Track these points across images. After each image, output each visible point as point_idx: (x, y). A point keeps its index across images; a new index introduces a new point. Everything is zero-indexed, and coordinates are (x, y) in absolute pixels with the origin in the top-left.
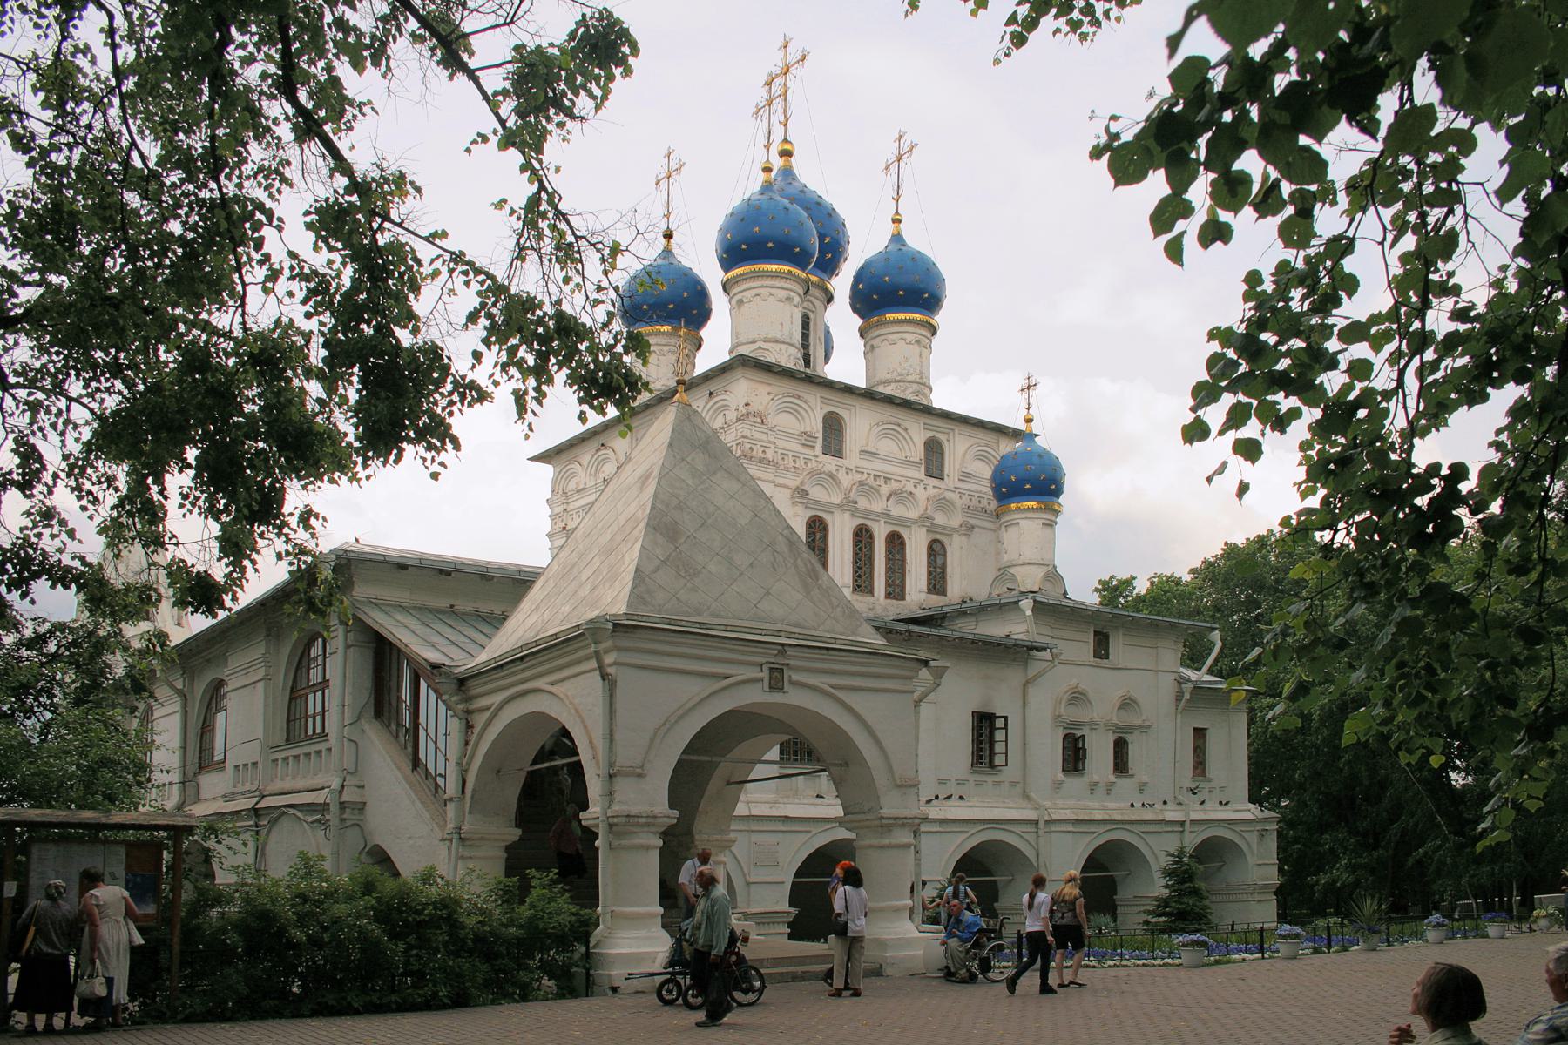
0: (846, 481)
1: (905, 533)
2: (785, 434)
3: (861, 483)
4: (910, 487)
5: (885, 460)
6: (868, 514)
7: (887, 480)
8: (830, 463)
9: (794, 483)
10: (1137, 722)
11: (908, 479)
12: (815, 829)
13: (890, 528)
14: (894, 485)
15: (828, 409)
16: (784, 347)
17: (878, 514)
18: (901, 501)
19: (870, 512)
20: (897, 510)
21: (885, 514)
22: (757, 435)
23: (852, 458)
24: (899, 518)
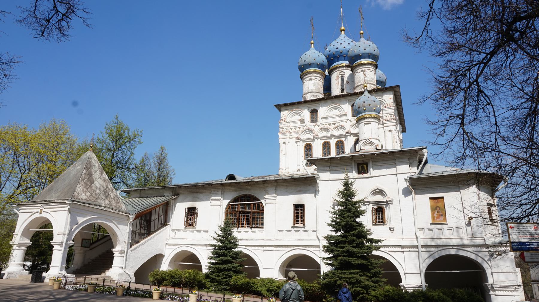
0: (316, 129)
1: (343, 139)
2: (294, 122)
3: (321, 129)
4: (343, 123)
7: (334, 124)
9: (296, 136)
10: (385, 200)
11: (342, 121)
12: (175, 247)
14: (337, 125)
15: (311, 109)
19: (326, 137)
20: (336, 133)
21: (332, 136)
23: (320, 121)
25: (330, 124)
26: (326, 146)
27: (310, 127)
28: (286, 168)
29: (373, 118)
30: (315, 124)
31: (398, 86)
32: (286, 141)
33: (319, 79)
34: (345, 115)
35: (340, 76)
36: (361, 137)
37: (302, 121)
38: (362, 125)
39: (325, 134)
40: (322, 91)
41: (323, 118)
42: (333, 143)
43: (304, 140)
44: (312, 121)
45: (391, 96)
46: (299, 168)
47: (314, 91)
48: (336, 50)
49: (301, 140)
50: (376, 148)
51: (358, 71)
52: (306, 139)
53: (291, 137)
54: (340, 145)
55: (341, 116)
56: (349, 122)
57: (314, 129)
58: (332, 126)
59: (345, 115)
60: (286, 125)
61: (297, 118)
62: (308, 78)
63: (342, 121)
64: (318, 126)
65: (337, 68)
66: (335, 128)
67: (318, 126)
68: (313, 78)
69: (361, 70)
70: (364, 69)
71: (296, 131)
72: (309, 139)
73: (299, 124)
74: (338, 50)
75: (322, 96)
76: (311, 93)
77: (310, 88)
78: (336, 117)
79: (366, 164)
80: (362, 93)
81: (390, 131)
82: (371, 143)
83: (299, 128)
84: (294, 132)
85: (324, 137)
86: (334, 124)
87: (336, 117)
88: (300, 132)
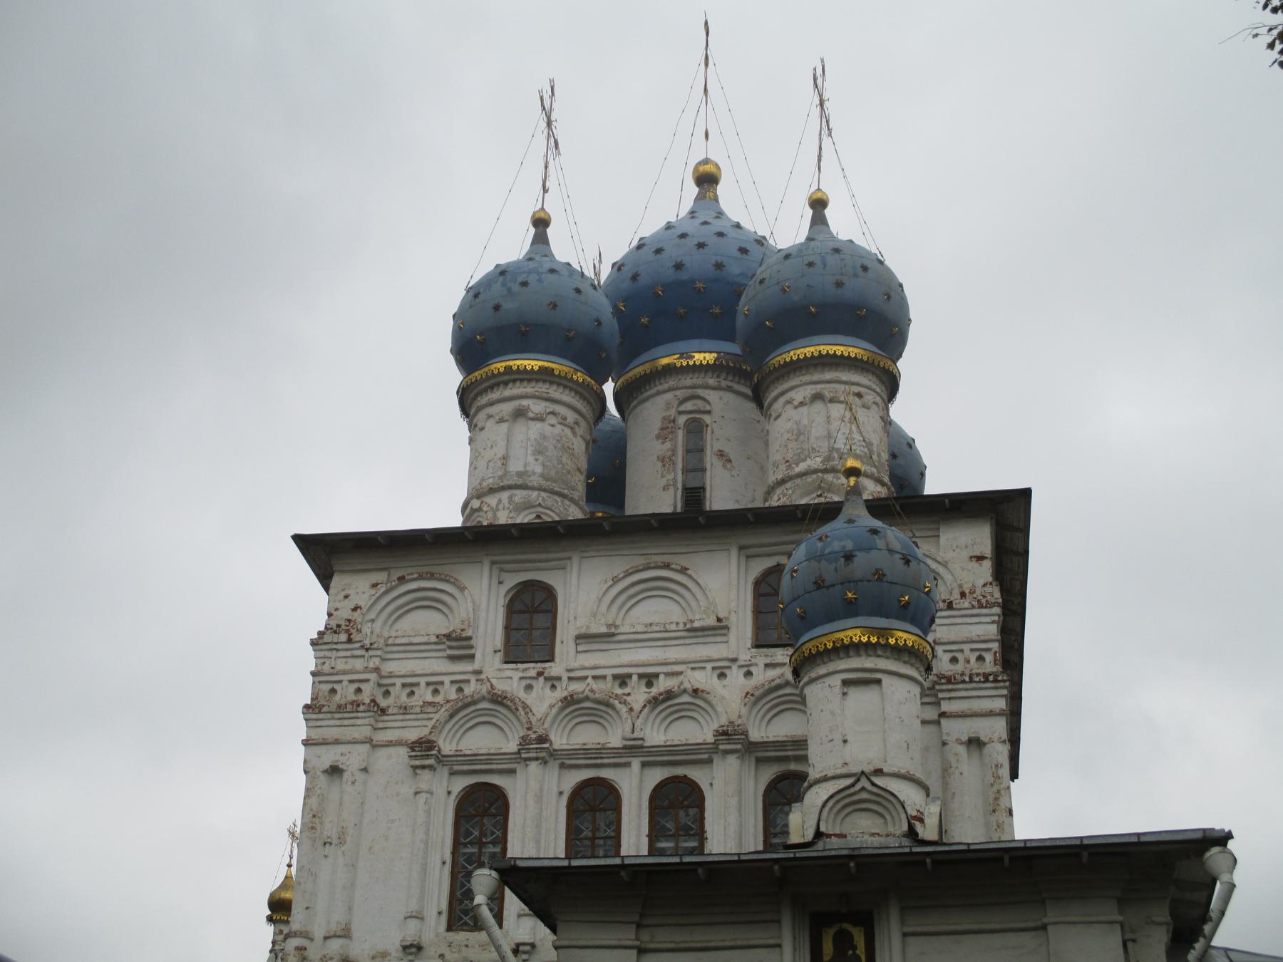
0: (542, 701)
1: (697, 774)
2: (411, 648)
4: (701, 679)
5: (637, 640)
6: (595, 755)
8: (510, 680)
9: (412, 735)
11: (697, 665)
13: (657, 776)
14: (663, 684)
15: (513, 580)
16: (505, 495)
17: (616, 752)
18: (681, 713)
20: (656, 735)
21: (634, 748)
22: (340, 665)
23: (566, 656)
24: (670, 749)
25: (623, 680)
26: (593, 805)
27: (500, 686)
28: (334, 927)
29: (899, 651)
30: (532, 669)
31: (1026, 494)
32: (353, 758)
33: (571, 416)
34: (720, 628)
35: (682, 420)
36: (821, 760)
37: (458, 645)
38: (824, 692)
39: (588, 736)
40: (580, 492)
41: (582, 638)
42: (635, 789)
43: (454, 764)
44: (514, 653)
45: (986, 547)
46: (411, 931)
47: (535, 481)
48: (670, 275)
49: (442, 759)
50: (912, 833)
51: (798, 396)
52: (474, 758)
53: (381, 737)
54: (678, 802)
55: (696, 632)
56: (736, 675)
57: (530, 699)
58: (639, 695)
59: (720, 628)
60: (359, 664)
61: (426, 624)
62: (507, 408)
63: (697, 665)
64: (553, 682)
65: (670, 370)
66: (654, 702)
67: (553, 682)
68: (537, 407)
69: (808, 391)
70: (827, 390)
71: (416, 701)
72: (490, 757)
73: (436, 664)
74: (684, 276)
75: (575, 513)
76: (519, 495)
77: (515, 466)
78: (663, 636)
79: (867, 922)
80: (829, 512)
81: (975, 743)
82: (883, 802)
83: (436, 688)
84: (405, 710)
85: (585, 752)
86: (649, 679)
87: (663, 636)
88: (442, 714)
